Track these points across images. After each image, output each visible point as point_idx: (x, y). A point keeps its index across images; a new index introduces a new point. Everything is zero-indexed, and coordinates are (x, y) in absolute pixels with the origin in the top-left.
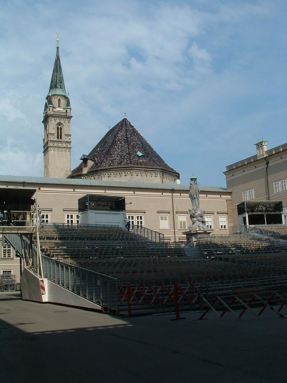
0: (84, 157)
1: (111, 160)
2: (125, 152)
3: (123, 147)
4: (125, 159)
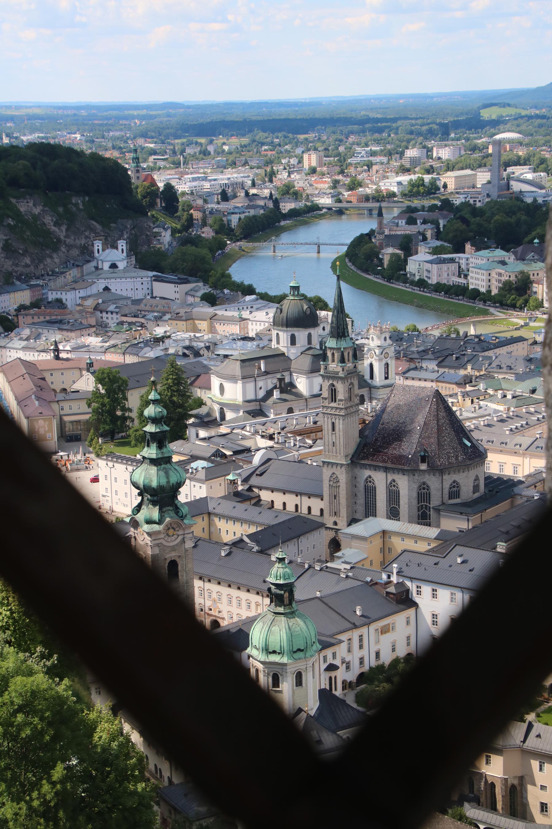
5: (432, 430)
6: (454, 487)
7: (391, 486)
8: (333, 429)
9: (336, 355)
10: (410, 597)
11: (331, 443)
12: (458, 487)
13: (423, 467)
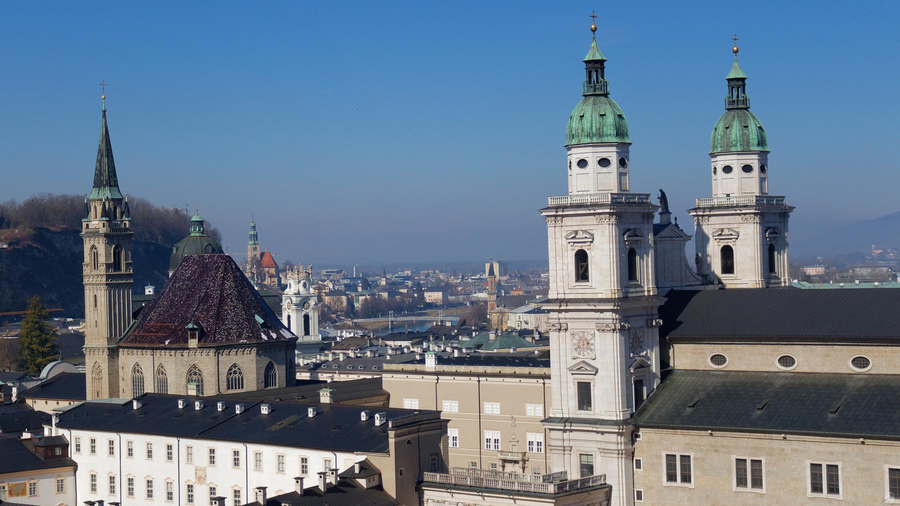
0: (193, 325)
1: (226, 330)
2: (241, 316)
3: (236, 308)
4: (244, 328)
5: (213, 302)
6: (235, 372)
7: (159, 373)
8: (96, 306)
9: (98, 208)
10: (69, 456)
11: (93, 323)
12: (240, 373)
13: (193, 343)
